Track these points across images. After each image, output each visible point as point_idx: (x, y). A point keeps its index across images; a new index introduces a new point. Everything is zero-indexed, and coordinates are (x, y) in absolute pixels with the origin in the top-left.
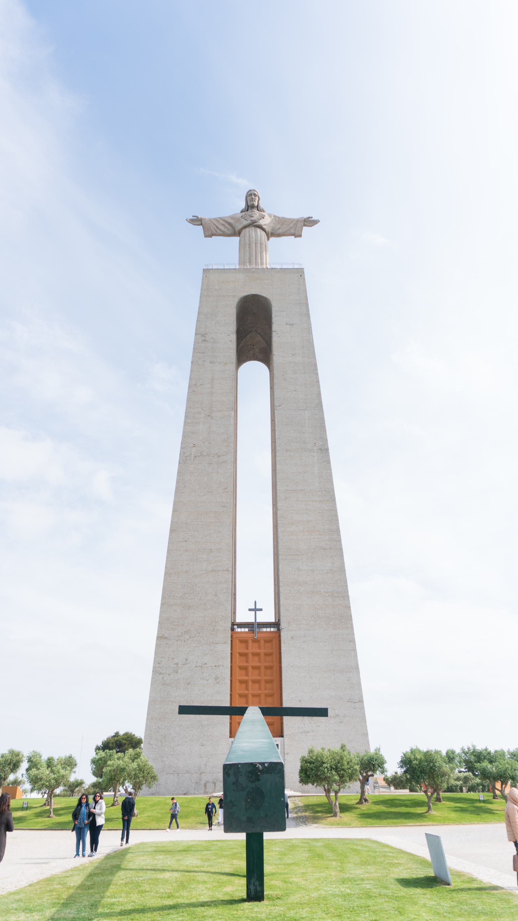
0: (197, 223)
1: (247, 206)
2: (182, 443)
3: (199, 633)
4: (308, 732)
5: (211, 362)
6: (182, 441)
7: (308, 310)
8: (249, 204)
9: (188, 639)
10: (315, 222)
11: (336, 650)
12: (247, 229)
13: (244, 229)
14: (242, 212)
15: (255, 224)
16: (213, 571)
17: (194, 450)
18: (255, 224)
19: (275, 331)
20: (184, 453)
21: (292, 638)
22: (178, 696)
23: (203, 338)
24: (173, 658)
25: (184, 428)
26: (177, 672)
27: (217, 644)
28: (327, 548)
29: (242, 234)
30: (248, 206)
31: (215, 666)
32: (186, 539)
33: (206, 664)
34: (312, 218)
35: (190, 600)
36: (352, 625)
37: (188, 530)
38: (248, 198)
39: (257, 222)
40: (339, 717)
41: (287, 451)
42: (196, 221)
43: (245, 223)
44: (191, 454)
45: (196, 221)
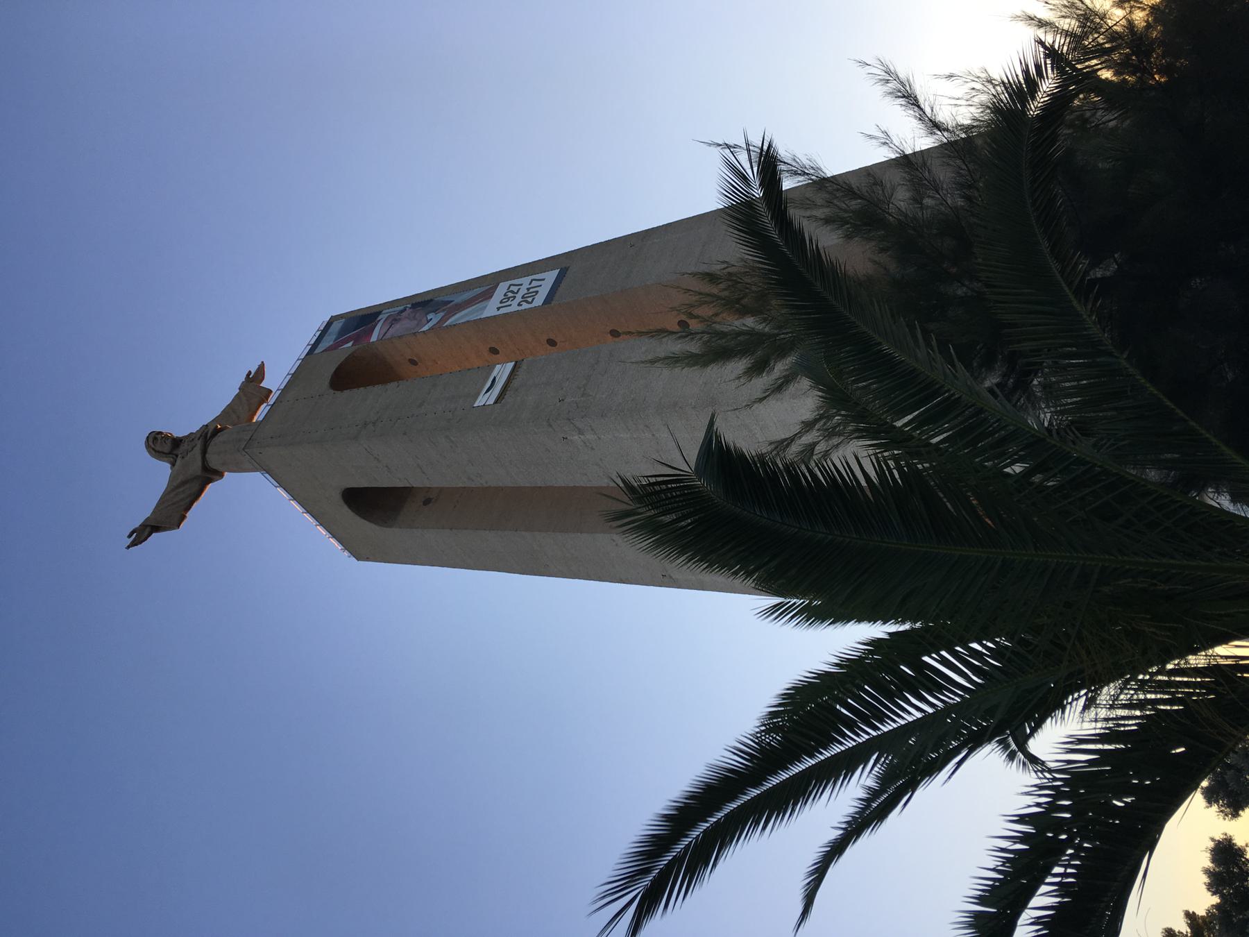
0: (146, 533)
1: (171, 456)
10: (261, 370)
12: (210, 449)
13: (207, 455)
14: (173, 465)
15: (209, 435)
18: (209, 435)
29: (214, 461)
30: (170, 453)
34: (250, 372)
38: (158, 448)
39: (208, 431)
42: (141, 534)
43: (198, 450)
45: (141, 534)
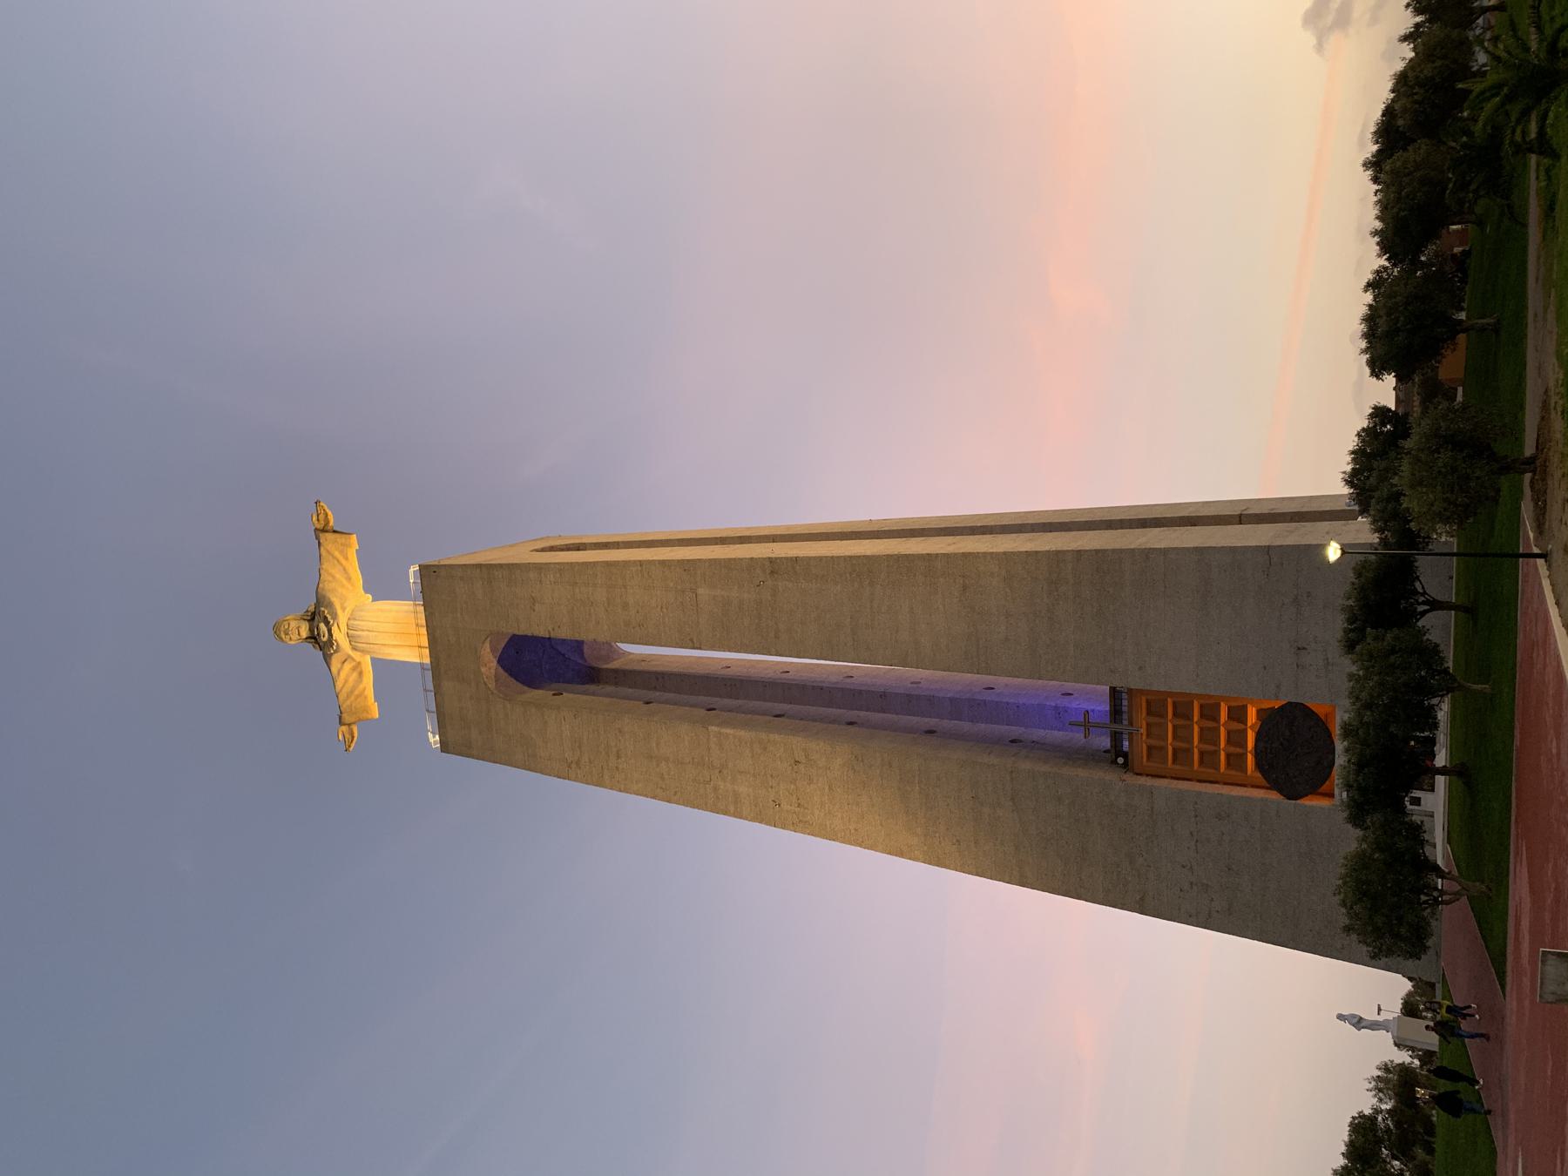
1: (309, 640)
2: (775, 826)
3: (1132, 838)
4: (1327, 659)
5: (618, 757)
6: (771, 825)
7: (501, 566)
8: (305, 637)
9: (1145, 860)
11: (1165, 587)
16: (1012, 799)
17: (785, 806)
19: (549, 632)
20: (793, 823)
21: (1140, 668)
22: (1252, 890)
23: (573, 766)
24: (1181, 890)
25: (746, 819)
26: (1207, 885)
27: (1152, 808)
28: (961, 582)
31: (1196, 816)
32: (954, 841)
33: (1191, 833)
35: (1071, 847)
36: (1114, 551)
37: (937, 835)
40: (1299, 597)
41: (777, 637)
44: (795, 812)
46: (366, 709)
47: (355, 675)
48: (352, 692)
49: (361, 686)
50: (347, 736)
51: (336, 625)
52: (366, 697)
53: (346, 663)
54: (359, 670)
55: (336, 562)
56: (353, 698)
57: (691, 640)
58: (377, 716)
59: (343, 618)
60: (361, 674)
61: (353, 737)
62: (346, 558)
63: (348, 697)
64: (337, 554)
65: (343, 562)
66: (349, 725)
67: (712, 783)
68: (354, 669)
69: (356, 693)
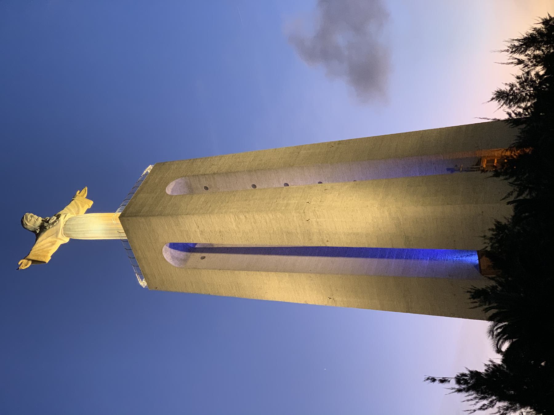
46: (45, 256)
47: (50, 244)
48: (43, 249)
49: (50, 248)
50: (23, 264)
51: (65, 215)
52: (48, 253)
53: (49, 238)
54: (53, 243)
55: (76, 207)
56: (41, 251)
57: (290, 165)
58: (47, 262)
59: (69, 216)
60: (53, 244)
61: (26, 265)
62: (83, 207)
63: (38, 250)
64: (80, 205)
65: (80, 207)
66: (29, 260)
67: (277, 202)
68: (50, 242)
69: (45, 250)
